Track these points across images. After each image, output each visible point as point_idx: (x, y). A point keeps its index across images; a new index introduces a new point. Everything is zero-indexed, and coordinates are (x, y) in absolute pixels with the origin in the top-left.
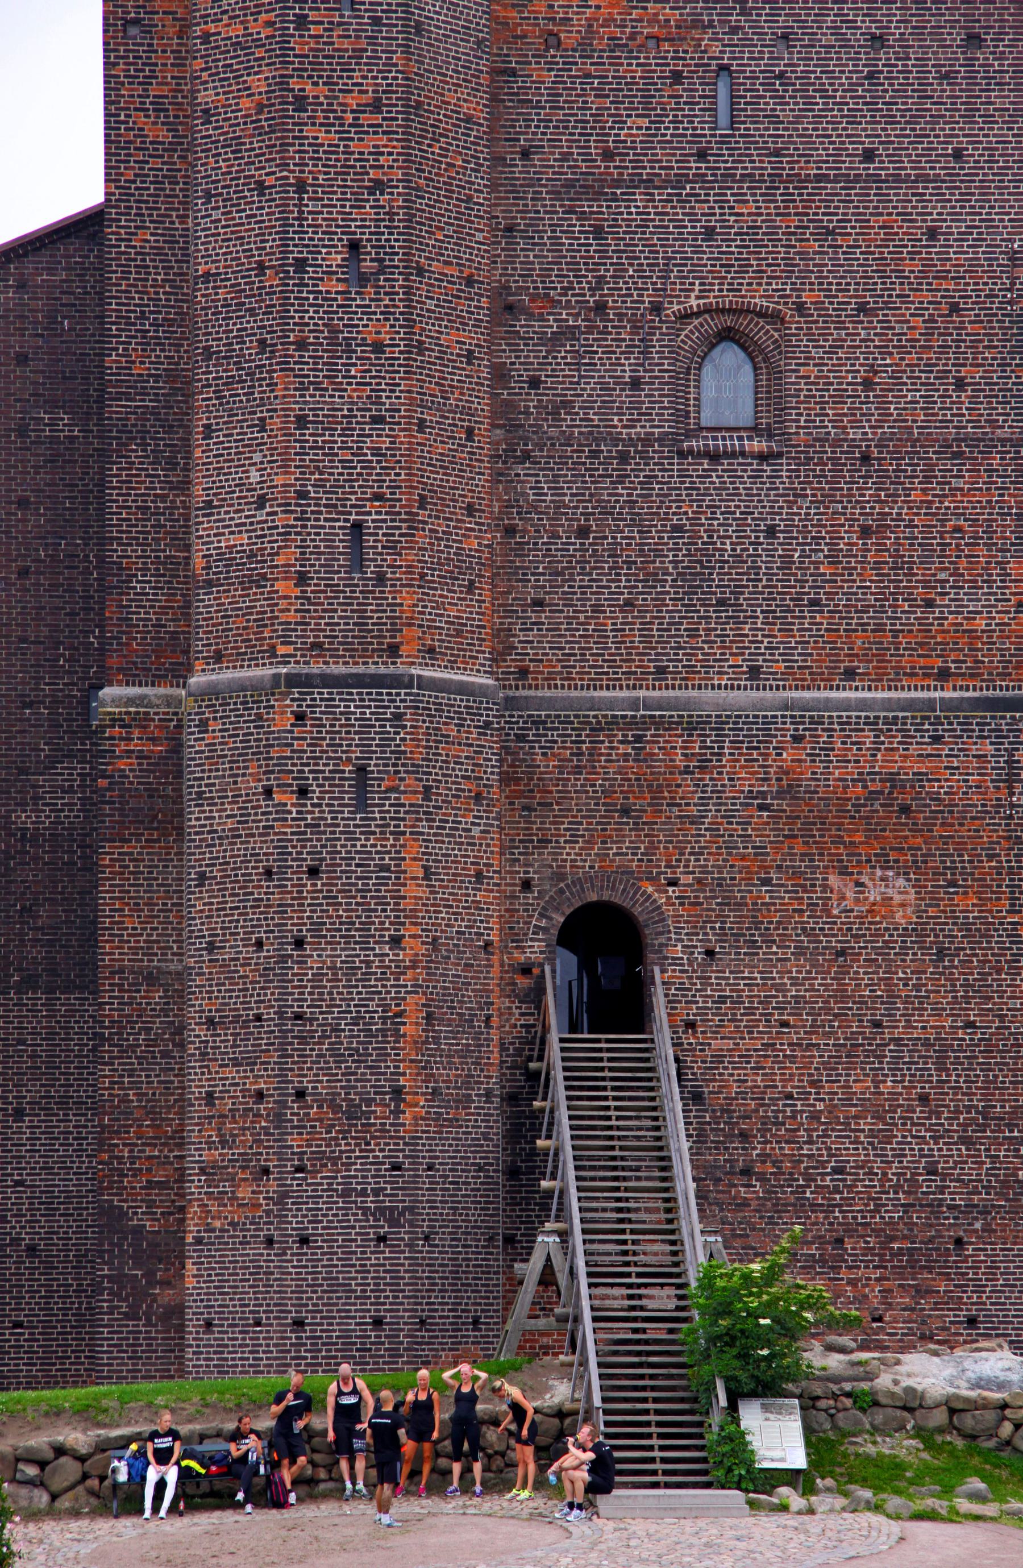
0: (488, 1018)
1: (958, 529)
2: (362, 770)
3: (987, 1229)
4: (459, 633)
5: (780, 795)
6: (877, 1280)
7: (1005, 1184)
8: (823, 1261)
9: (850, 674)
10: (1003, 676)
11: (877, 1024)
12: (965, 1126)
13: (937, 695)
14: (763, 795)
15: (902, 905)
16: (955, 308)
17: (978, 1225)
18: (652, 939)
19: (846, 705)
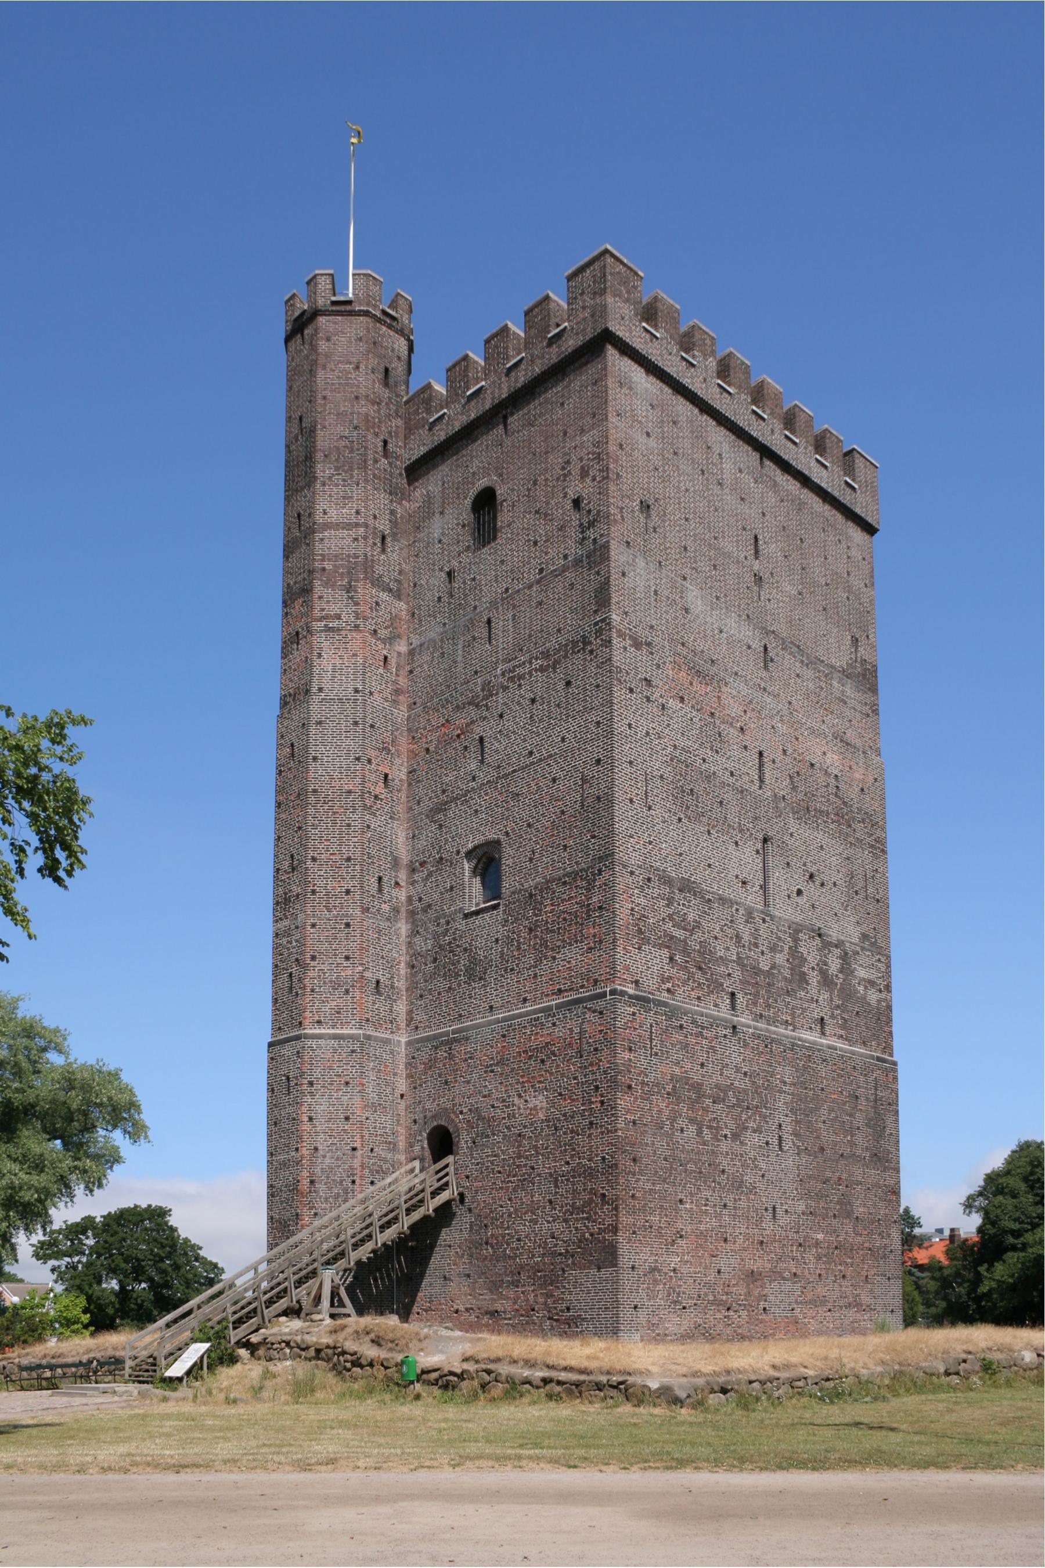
0: (353, 1182)
1: (565, 919)
2: (288, 1079)
3: (573, 1263)
4: (338, 1013)
5: (497, 1064)
6: (533, 1291)
7: (580, 1241)
8: (513, 1282)
9: (525, 1000)
10: (582, 987)
11: (533, 1168)
12: (565, 1214)
13: (554, 1003)
14: (491, 1065)
15: (541, 1108)
16: (563, 812)
17: (570, 1262)
18: (455, 1140)
19: (520, 1016)
